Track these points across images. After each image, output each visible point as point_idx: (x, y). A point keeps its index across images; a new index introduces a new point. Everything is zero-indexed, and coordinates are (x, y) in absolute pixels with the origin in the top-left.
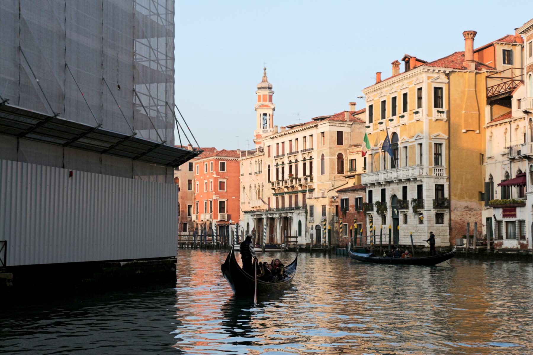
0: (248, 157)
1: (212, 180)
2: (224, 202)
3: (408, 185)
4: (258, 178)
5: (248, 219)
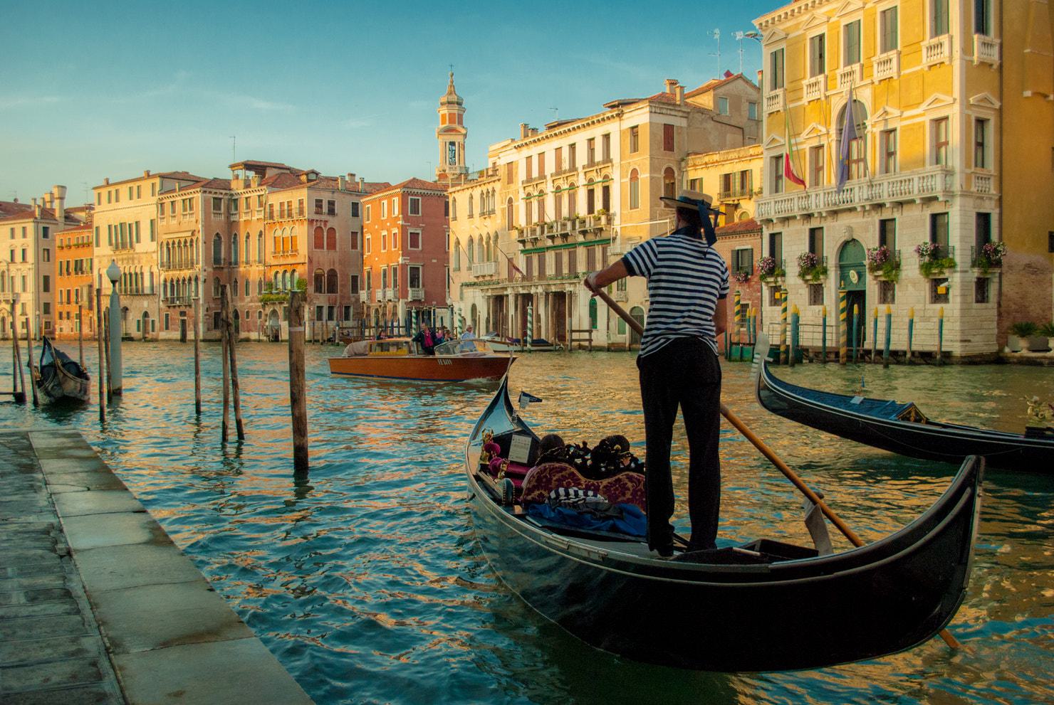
0: (466, 186)
1: (395, 230)
2: (418, 268)
3: (896, 215)
4: (488, 222)
5: (474, 297)
